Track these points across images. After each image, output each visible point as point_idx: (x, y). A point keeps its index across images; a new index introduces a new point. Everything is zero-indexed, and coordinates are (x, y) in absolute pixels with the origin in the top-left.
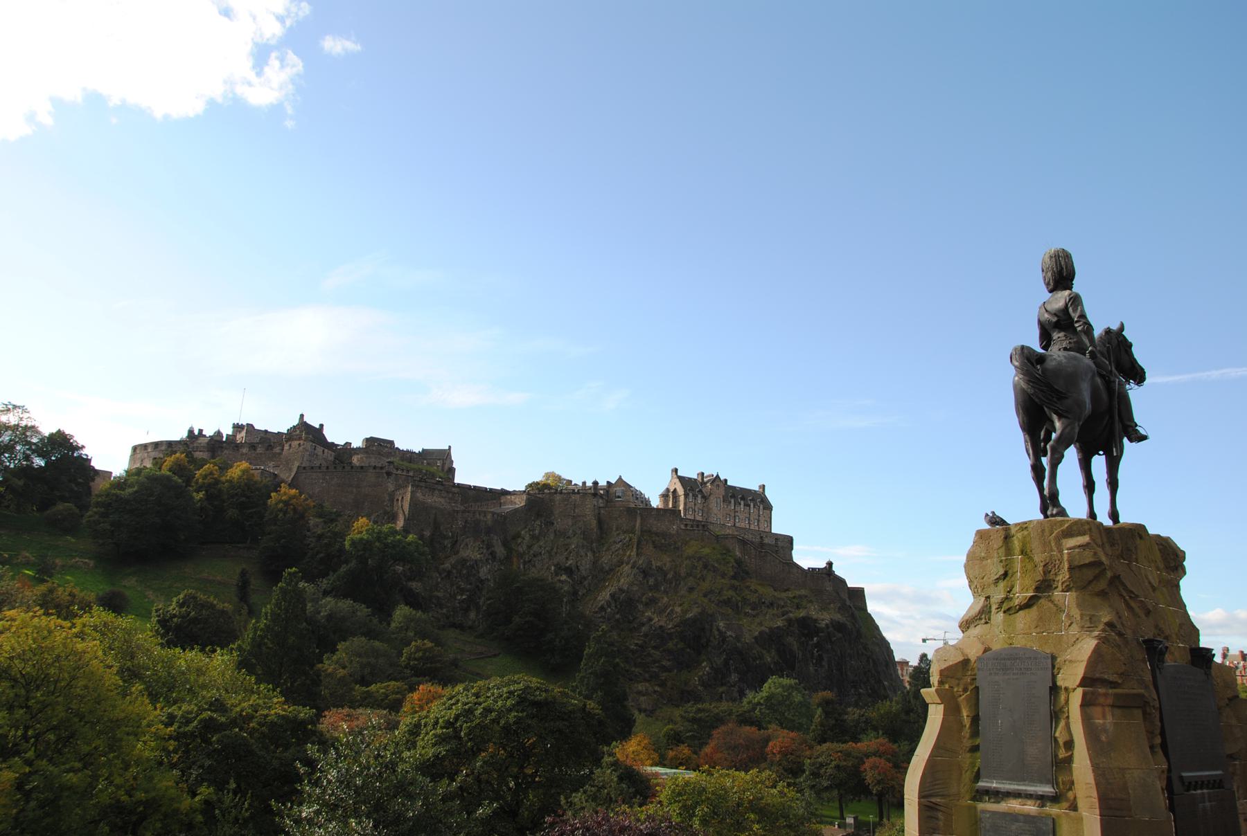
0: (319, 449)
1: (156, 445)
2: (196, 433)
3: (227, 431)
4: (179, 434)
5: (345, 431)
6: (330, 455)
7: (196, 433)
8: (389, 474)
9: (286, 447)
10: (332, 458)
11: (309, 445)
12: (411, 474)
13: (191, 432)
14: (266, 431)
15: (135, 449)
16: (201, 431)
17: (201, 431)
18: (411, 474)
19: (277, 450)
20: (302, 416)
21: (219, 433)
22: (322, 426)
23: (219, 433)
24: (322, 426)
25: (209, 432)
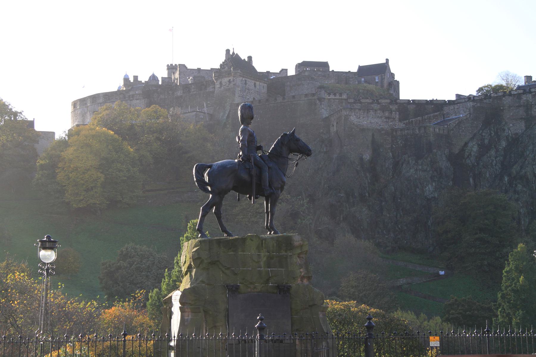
0: (251, 83)
1: (94, 98)
2: (132, 80)
3: (162, 74)
4: (114, 85)
5: (276, 57)
6: (262, 87)
7: (132, 80)
8: (320, 99)
9: (217, 86)
10: (265, 90)
11: (239, 81)
12: (344, 96)
13: (126, 80)
14: (199, 70)
15: (75, 104)
16: (136, 78)
17: (136, 78)
18: (344, 96)
19: (210, 89)
20: (228, 51)
21: (153, 78)
22: (250, 58)
23: (153, 78)
24: (250, 58)
25: (144, 78)
